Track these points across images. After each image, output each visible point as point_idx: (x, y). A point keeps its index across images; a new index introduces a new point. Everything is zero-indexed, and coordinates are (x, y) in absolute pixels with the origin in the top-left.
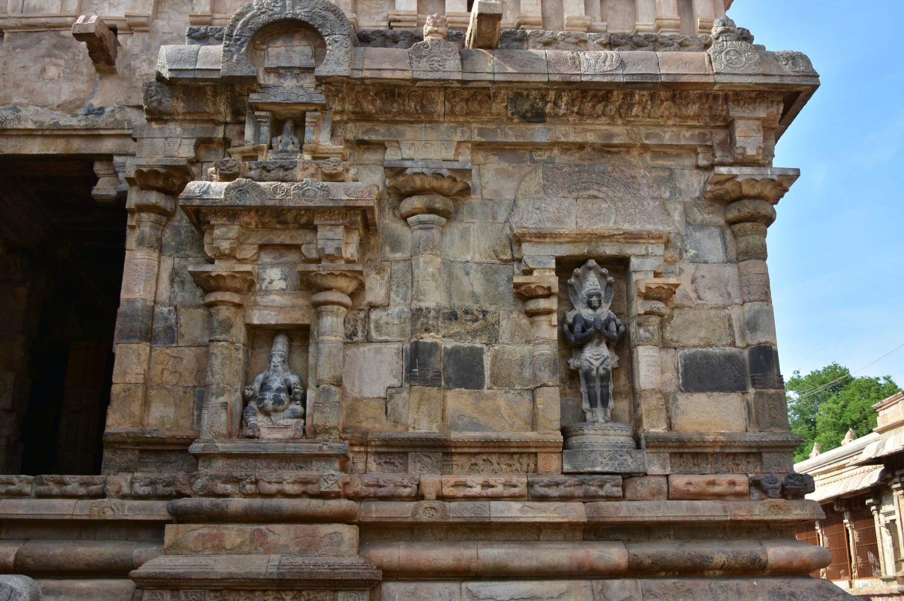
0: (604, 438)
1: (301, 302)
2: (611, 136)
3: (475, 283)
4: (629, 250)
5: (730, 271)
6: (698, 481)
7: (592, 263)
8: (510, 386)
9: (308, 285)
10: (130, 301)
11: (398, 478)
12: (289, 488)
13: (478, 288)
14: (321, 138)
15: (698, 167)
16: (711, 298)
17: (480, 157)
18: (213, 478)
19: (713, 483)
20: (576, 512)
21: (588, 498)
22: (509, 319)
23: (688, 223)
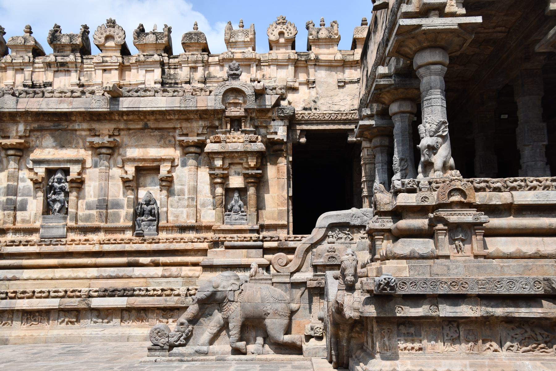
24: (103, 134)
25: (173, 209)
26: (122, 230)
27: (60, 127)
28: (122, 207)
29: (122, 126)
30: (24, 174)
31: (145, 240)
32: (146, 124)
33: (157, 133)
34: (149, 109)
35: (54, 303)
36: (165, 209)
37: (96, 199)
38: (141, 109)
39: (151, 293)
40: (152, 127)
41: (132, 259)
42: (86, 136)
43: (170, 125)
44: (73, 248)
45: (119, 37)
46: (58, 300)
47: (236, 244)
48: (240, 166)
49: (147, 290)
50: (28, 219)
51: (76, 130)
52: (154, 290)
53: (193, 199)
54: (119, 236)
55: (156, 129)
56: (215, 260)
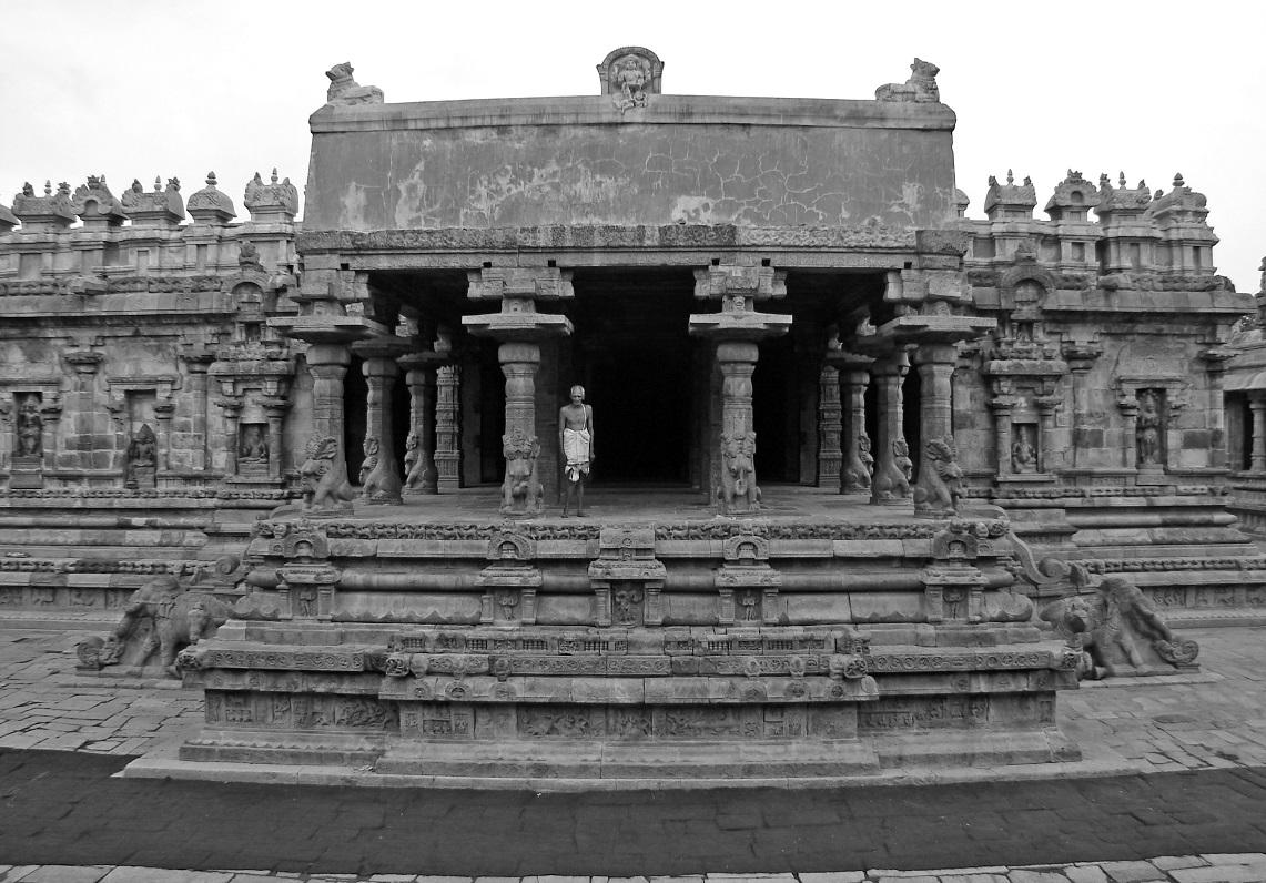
0: (1153, 473)
1: (1034, 413)
2: (1162, 330)
3: (1099, 400)
4: (1166, 386)
5: (1207, 394)
6: (1189, 488)
7: (1150, 391)
8: (1114, 446)
9: (1040, 407)
10: (958, 411)
11: (1073, 488)
12: (1038, 495)
13: (1101, 402)
14: (1040, 335)
15: (1196, 343)
16: (1199, 406)
17: (1103, 338)
18: (1008, 492)
19: (1194, 489)
20: (1142, 502)
21: (1145, 496)
22: (1114, 417)
23: (1191, 371)
26: (110, 478)
27: (29, 335)
28: (110, 447)
32: (137, 331)
33: (152, 342)
35: (22, 578)
36: (164, 451)
39: (139, 569)
42: (63, 346)
43: (169, 332)
44: (47, 502)
46: (28, 574)
47: (252, 503)
48: (258, 393)
49: (134, 566)
52: (143, 566)
53: (199, 437)
54: (109, 487)
56: (223, 525)
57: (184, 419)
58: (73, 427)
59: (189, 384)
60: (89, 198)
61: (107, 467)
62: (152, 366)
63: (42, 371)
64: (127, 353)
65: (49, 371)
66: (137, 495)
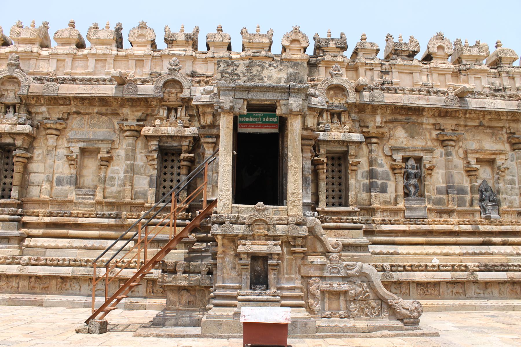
24: (447, 128)
25: (508, 196)
28: (467, 193)
29: (462, 123)
30: (382, 160)
31: (491, 222)
32: (481, 122)
33: (488, 130)
34: (493, 110)
35: (447, 276)
37: (444, 185)
38: (487, 109)
40: (486, 125)
41: (487, 239)
43: (501, 125)
45: (449, 48)
46: (449, 273)
50: (388, 200)
51: (422, 124)
55: (490, 127)
57: (511, 178)
58: (440, 180)
59: (512, 156)
60: (439, 44)
61: (466, 206)
62: (489, 145)
63: (419, 143)
64: (474, 136)
65: (424, 144)
66: (491, 223)
